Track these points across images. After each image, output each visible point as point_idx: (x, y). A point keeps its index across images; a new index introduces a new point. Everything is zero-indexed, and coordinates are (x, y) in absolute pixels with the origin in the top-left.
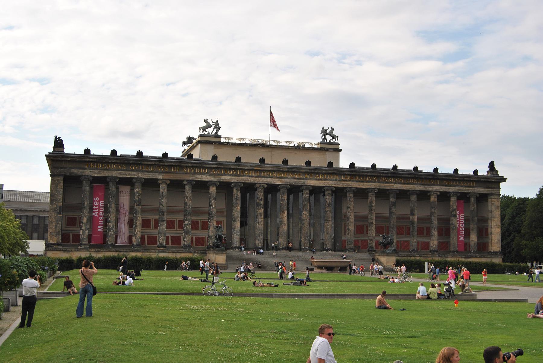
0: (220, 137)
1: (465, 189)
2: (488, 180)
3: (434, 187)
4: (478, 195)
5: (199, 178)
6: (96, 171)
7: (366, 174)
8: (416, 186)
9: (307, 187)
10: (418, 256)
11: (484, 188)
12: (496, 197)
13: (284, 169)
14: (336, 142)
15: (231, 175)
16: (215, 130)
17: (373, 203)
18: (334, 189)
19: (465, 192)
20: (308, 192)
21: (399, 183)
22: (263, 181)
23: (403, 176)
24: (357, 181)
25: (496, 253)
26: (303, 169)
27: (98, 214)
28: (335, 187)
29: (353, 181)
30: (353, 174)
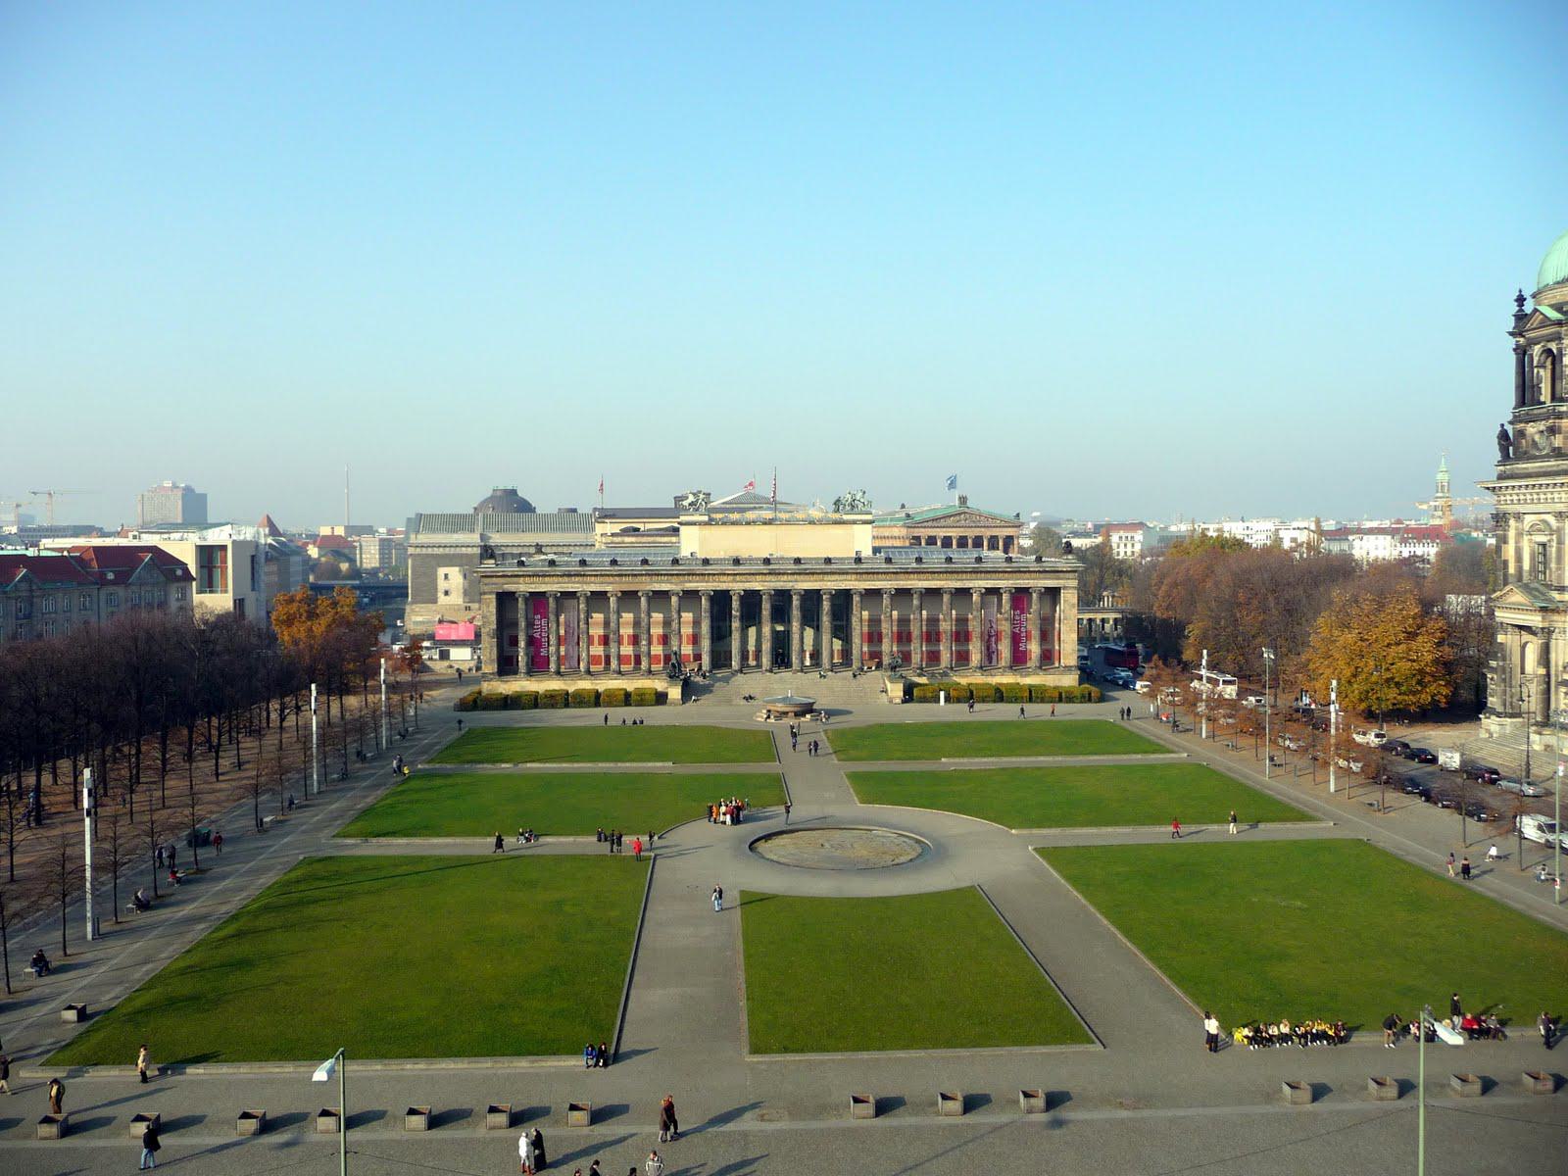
5: (657, 587)
6: (533, 586)
8: (949, 582)
11: (1053, 579)
13: (765, 572)
15: (697, 582)
18: (834, 592)
22: (737, 586)
25: (1068, 668)
27: (540, 635)
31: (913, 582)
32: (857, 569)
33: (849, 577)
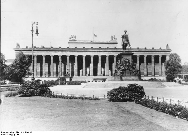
0: (76, 41)
14: (116, 40)
16: (75, 39)
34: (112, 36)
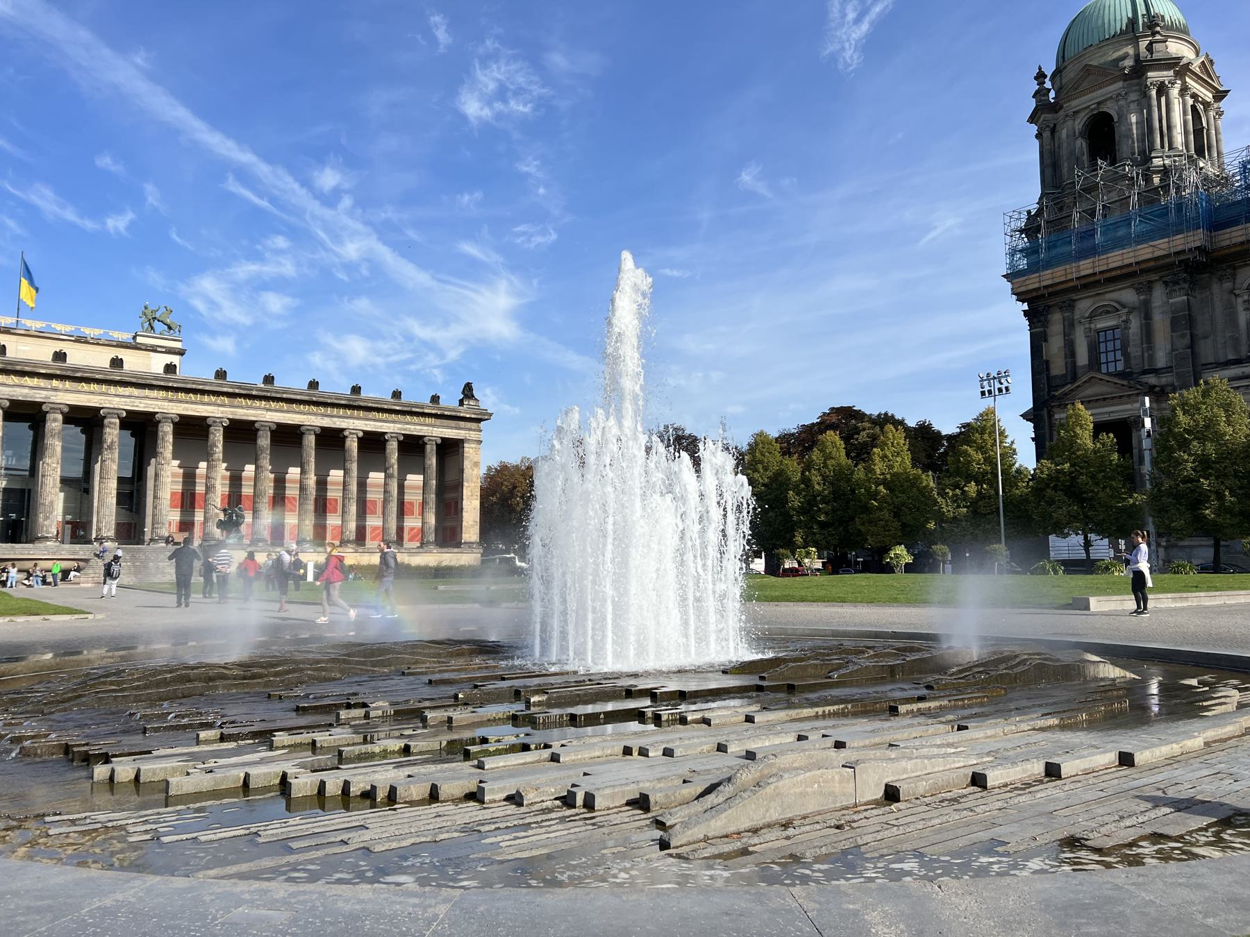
1: (415, 427)
2: (458, 414)
3: (352, 421)
4: (439, 441)
7: (201, 387)
8: (313, 418)
9: (56, 408)
10: (312, 550)
11: (451, 428)
12: (473, 446)
17: (217, 447)
19: (415, 433)
20: (60, 417)
21: (276, 411)
23: (285, 396)
24: (181, 402)
25: (469, 544)
26: (45, 366)
28: (127, 411)
29: (171, 401)
30: (170, 385)
31: (259, 412)
32: (168, 380)
33: (155, 393)
34: (150, 308)
